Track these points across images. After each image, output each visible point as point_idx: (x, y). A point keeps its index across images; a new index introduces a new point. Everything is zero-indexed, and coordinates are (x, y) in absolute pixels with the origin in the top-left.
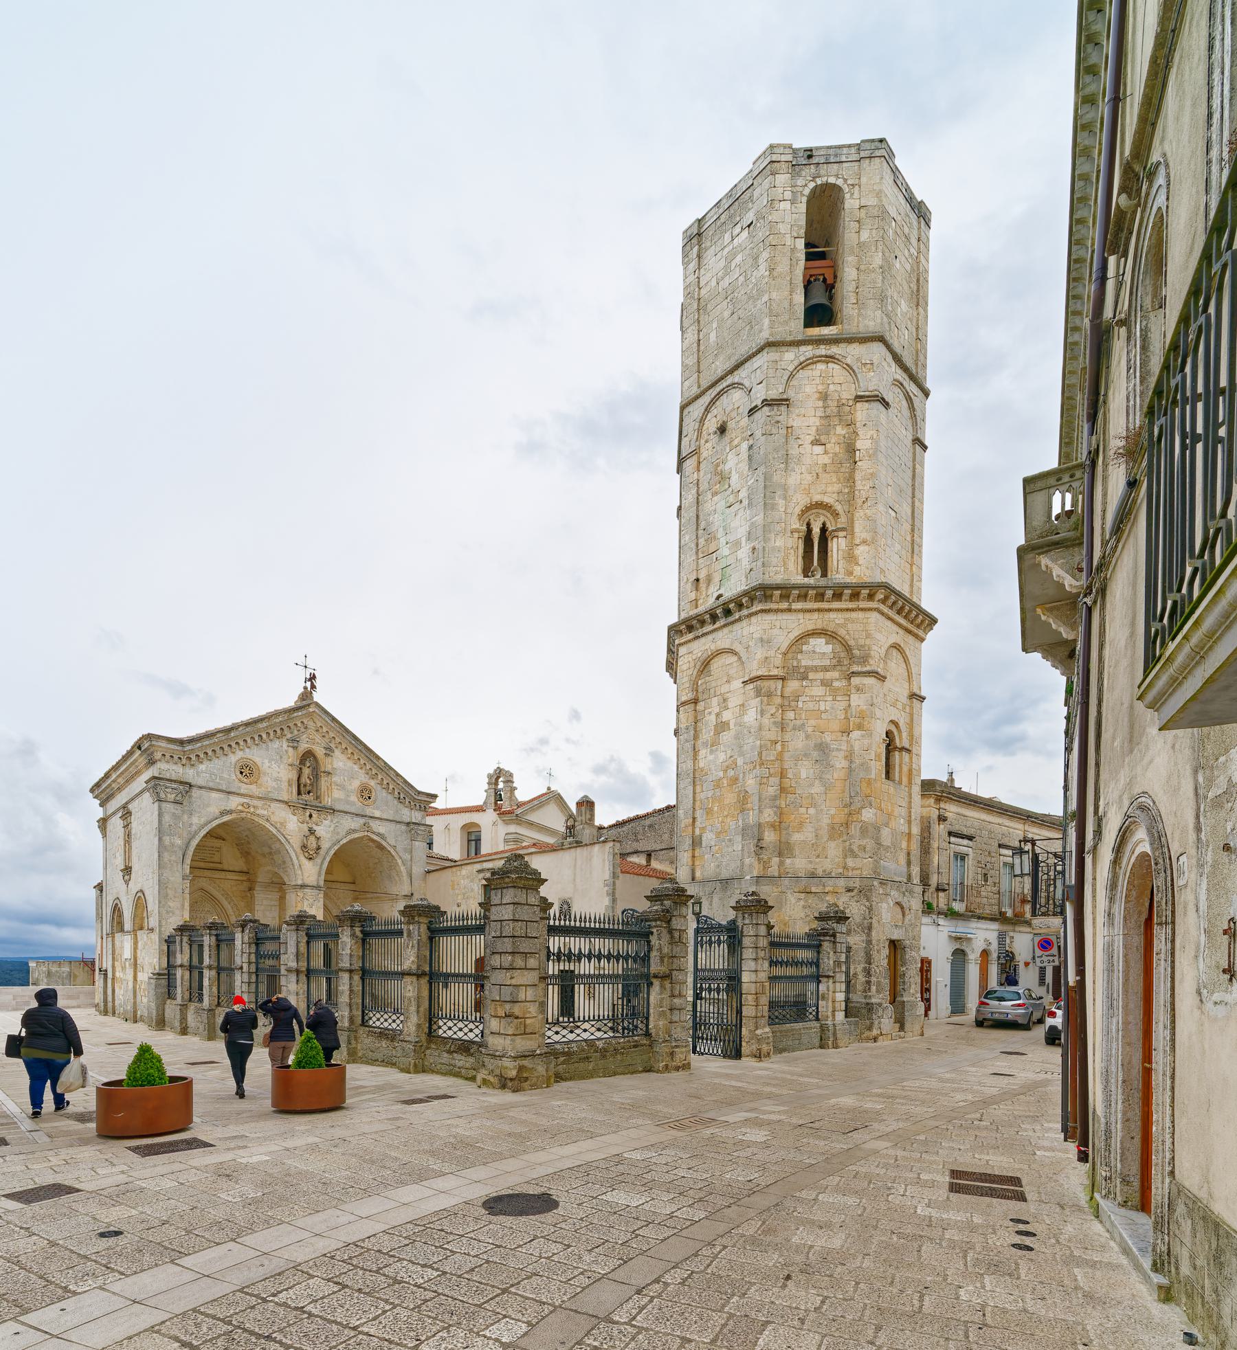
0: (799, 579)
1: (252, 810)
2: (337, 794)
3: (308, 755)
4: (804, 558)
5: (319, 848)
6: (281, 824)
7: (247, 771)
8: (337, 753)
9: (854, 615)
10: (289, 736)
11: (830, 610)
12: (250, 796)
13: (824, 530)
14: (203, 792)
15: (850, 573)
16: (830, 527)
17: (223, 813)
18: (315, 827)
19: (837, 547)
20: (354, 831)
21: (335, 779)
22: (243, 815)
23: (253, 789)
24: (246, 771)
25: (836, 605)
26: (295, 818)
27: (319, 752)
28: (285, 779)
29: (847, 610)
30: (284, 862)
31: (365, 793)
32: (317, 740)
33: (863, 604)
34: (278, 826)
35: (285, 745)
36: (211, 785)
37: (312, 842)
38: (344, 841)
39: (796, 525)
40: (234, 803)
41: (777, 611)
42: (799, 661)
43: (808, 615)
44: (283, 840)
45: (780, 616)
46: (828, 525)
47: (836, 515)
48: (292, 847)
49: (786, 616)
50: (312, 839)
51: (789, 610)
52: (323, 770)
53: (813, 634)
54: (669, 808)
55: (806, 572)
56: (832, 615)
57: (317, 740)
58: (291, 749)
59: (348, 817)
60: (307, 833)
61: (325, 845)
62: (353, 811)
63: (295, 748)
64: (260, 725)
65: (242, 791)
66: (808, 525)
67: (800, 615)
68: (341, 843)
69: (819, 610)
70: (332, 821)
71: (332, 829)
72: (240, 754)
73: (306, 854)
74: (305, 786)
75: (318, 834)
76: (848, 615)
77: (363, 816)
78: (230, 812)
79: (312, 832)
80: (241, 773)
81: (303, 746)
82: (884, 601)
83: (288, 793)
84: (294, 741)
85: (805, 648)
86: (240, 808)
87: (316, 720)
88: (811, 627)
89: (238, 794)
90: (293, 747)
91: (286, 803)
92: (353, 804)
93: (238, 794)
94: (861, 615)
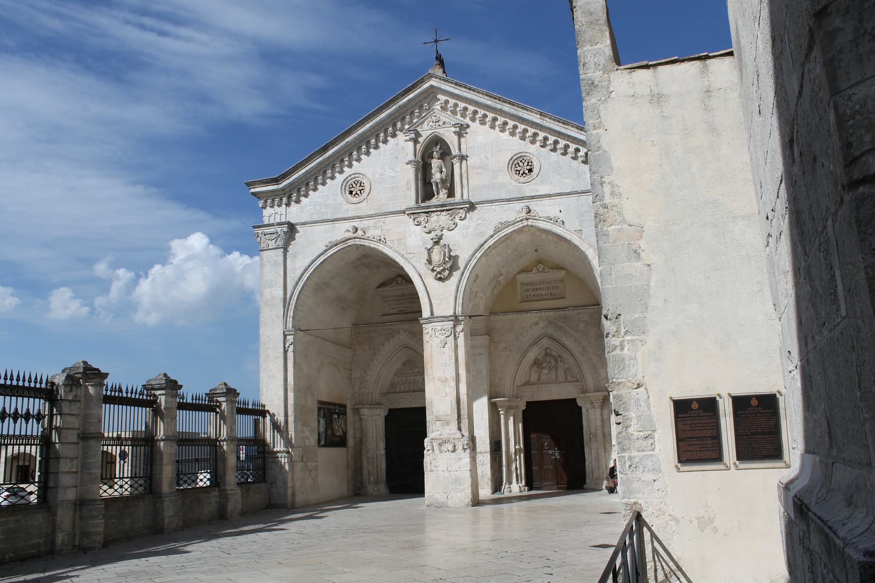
2: (475, 180)
6: (399, 240)
14: (307, 228)
20: (507, 225)
23: (364, 208)
32: (443, 119)
36: (316, 218)
38: (491, 242)
40: (341, 231)
57: (443, 119)
59: (494, 207)
62: (504, 197)
65: (350, 215)
68: (486, 246)
80: (351, 193)
83: (409, 197)
89: (345, 219)
90: (410, 140)
93: (345, 219)
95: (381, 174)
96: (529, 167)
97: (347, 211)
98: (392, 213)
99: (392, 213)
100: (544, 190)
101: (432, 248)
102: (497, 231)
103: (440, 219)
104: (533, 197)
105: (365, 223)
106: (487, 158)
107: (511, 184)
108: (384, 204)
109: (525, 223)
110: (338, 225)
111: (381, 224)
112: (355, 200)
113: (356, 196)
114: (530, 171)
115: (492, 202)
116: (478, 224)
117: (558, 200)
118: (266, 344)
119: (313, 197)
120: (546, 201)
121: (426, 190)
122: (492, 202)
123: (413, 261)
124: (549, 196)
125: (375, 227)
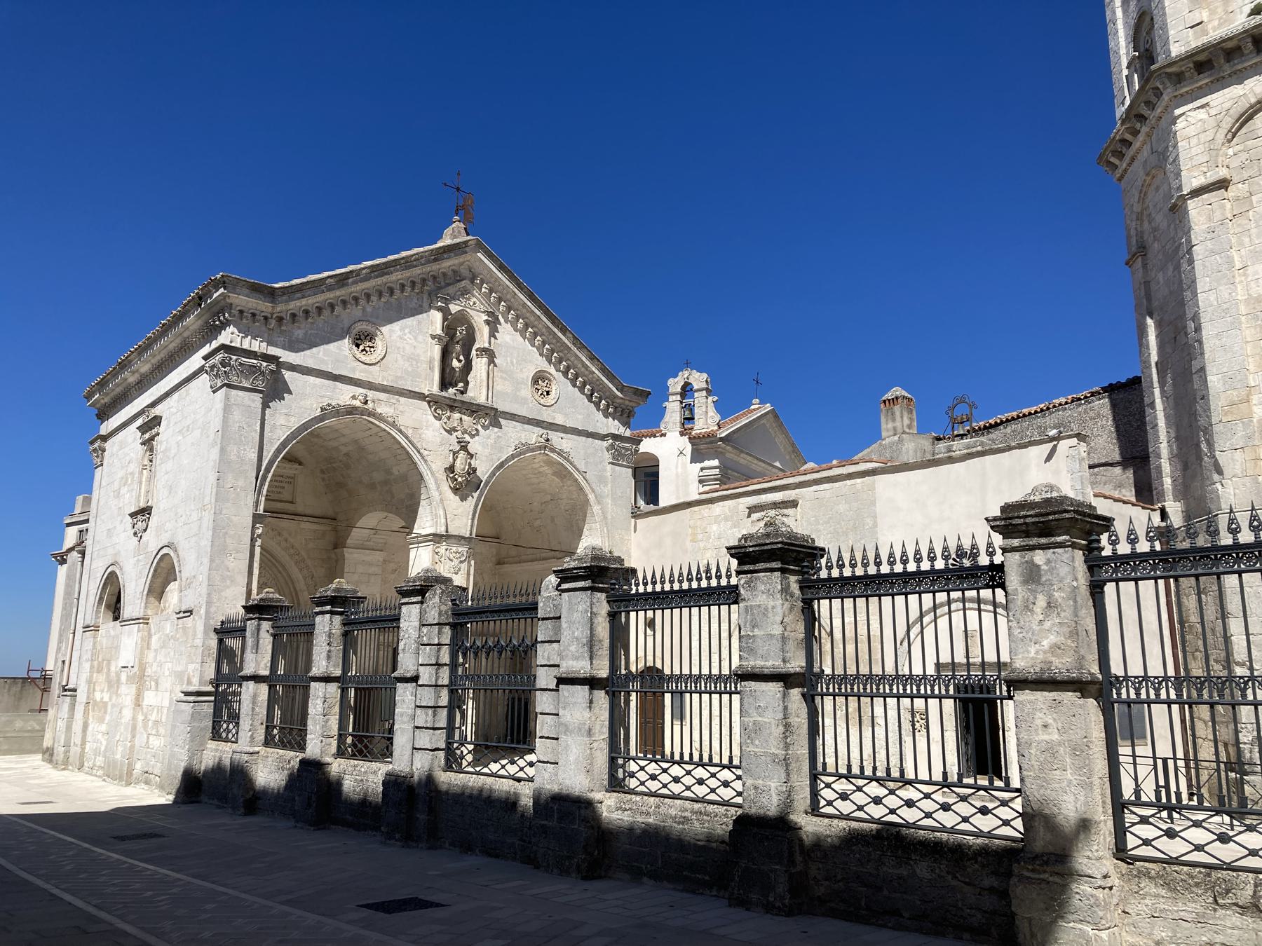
1: (370, 405)
34: (409, 432)
40: (345, 395)
65: (357, 376)
77: (538, 423)
92: (524, 401)
96: (547, 389)
97: (354, 369)
101: (458, 452)
106: (512, 362)
108: (400, 377)
111: (394, 401)
113: (364, 352)
114: (548, 393)
116: (498, 436)
118: (224, 528)
119: (310, 332)
123: (428, 459)
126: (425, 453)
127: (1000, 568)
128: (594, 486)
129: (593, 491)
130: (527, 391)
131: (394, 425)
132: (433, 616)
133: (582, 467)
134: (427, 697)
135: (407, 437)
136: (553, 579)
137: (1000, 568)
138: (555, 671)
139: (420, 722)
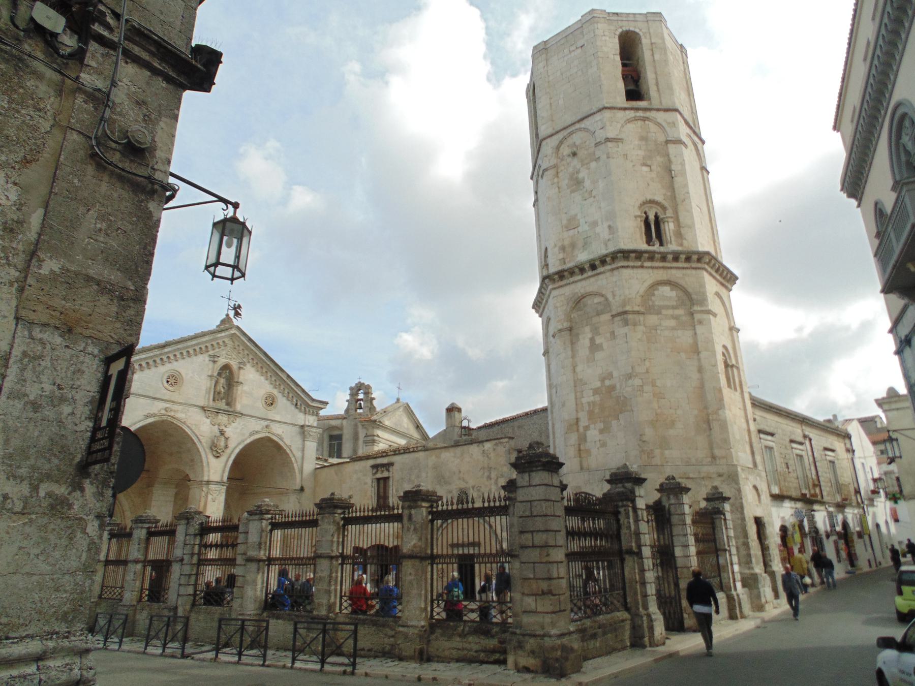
0: (644, 246)
1: (172, 414)
3: (226, 367)
4: (645, 234)
5: (226, 447)
7: (174, 380)
8: (248, 366)
9: (688, 272)
10: (211, 352)
11: (671, 268)
12: (173, 402)
13: (656, 217)
15: (681, 245)
16: (661, 216)
17: (147, 417)
18: (225, 429)
19: (669, 228)
21: (245, 388)
22: (165, 418)
23: (175, 397)
24: (172, 381)
25: (675, 264)
26: (208, 421)
27: (234, 364)
28: (204, 388)
29: (683, 268)
30: (192, 460)
31: (270, 402)
33: (694, 265)
34: (193, 428)
35: (207, 359)
37: (222, 443)
39: (639, 213)
41: (633, 267)
42: (653, 302)
43: (655, 271)
44: (196, 440)
45: (635, 271)
46: (659, 214)
47: (664, 209)
48: (203, 446)
49: (640, 271)
50: (223, 439)
51: (642, 267)
52: (236, 380)
53: (661, 283)
54: (544, 410)
55: (649, 241)
56: (674, 272)
58: (211, 363)
59: (252, 420)
60: (218, 434)
61: (232, 444)
63: (214, 362)
64: (189, 343)
66: (645, 213)
67: (650, 271)
69: (663, 268)
70: (239, 424)
71: (238, 431)
72: (168, 367)
73: (215, 453)
74: (219, 393)
75: (227, 435)
76: (684, 271)
78: (153, 415)
79: (222, 433)
80: (168, 382)
81: (222, 361)
82: (708, 264)
84: (214, 359)
85: (656, 292)
86: (163, 412)
87: (234, 340)
88: (659, 279)
89: (162, 400)
91: (203, 408)
94: (694, 272)
95: (191, 377)
98: (195, 406)
99: (195, 406)
100: (278, 418)
102: (251, 434)
103: (223, 418)
104: (272, 421)
105: (176, 407)
107: (259, 408)
109: (267, 435)
110: (156, 403)
112: (170, 388)
115: (252, 416)
117: (282, 425)
120: (278, 425)
121: (217, 396)
122: (252, 416)
124: (280, 422)
125: (182, 412)
126: (201, 438)
127: (317, 520)
128: (294, 452)
129: (294, 456)
130: (260, 404)
131: (184, 423)
132: (192, 531)
133: (288, 443)
134: (187, 569)
135: (191, 429)
136: (246, 514)
137: (317, 520)
138: (244, 556)
139: (182, 582)
